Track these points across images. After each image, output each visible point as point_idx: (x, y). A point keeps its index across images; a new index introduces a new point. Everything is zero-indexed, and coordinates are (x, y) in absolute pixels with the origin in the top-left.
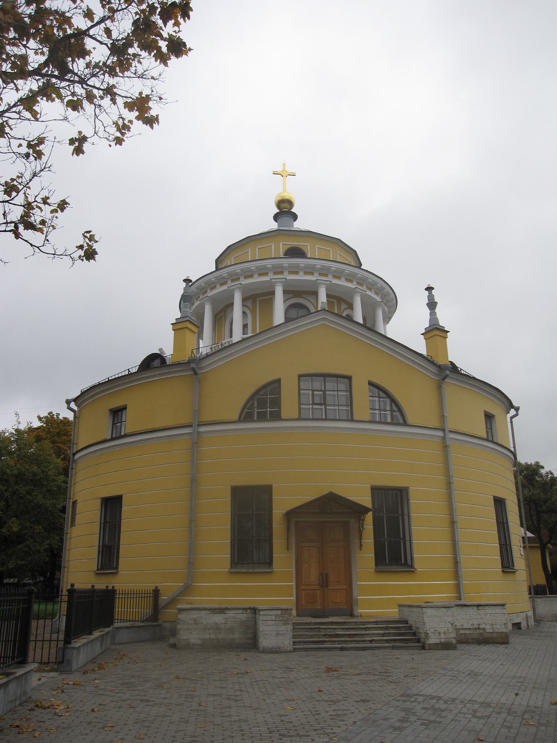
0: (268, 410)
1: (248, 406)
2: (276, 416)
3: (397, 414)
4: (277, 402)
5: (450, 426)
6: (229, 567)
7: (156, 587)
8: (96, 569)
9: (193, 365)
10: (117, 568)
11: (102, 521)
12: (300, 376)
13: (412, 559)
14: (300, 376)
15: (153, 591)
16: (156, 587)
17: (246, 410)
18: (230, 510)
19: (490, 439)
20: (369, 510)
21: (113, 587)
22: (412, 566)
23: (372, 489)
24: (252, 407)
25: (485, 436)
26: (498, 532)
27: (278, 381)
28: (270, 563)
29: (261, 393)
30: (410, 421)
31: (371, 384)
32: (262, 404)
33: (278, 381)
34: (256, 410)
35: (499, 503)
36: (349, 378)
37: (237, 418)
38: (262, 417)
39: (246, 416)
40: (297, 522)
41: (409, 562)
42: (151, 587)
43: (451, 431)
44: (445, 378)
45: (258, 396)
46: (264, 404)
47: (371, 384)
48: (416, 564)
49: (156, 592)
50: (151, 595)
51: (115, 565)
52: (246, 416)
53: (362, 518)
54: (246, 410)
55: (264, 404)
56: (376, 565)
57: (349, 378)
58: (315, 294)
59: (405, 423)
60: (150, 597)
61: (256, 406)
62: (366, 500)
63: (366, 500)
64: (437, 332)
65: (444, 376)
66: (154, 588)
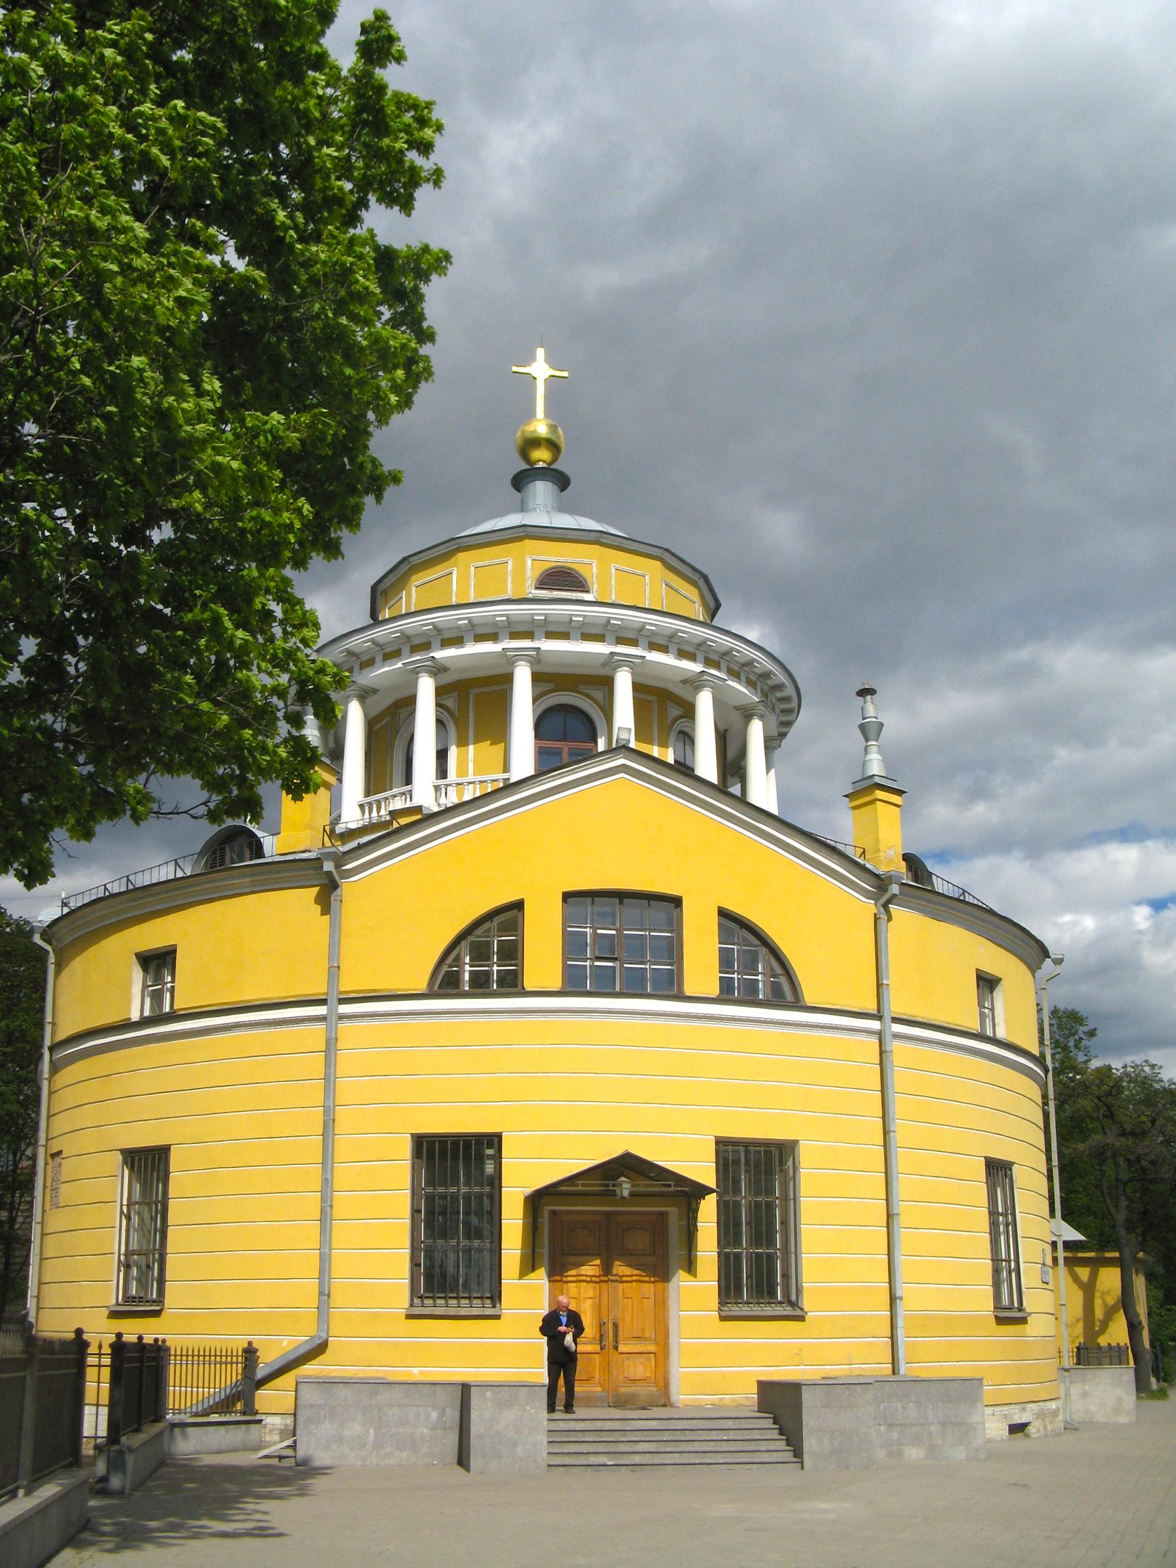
0: (495, 968)
1: (449, 960)
2: (512, 984)
3: (783, 980)
4: (513, 953)
5: (897, 1005)
6: (407, 1305)
7: (250, 1343)
8: (114, 1302)
9: (328, 866)
10: (160, 1300)
11: (125, 1202)
12: (567, 896)
13: (799, 1291)
14: (567, 896)
15: (246, 1351)
16: (250, 1343)
17: (445, 968)
18: (408, 1184)
19: (989, 1033)
20: (709, 1191)
21: (164, 1341)
22: (794, 1305)
23: (717, 1143)
24: (458, 960)
25: (974, 1026)
26: (990, 1233)
27: (519, 905)
28: (496, 1297)
29: (479, 931)
30: (809, 999)
31: (723, 913)
32: (480, 953)
33: (519, 905)
34: (467, 968)
35: (998, 1171)
36: (677, 902)
37: (422, 985)
38: (480, 985)
39: (445, 982)
40: (554, 1213)
41: (793, 1298)
42: (240, 1343)
43: (896, 1020)
44: (889, 901)
45: (471, 938)
46: (484, 956)
47: (723, 913)
48: (807, 1302)
49: (250, 1353)
50: (240, 1359)
51: (154, 1296)
52: (445, 982)
53: (694, 1206)
54: (445, 968)
55: (484, 956)
56: (722, 1303)
57: (677, 902)
58: (607, 684)
59: (797, 1004)
60: (237, 1363)
61: (467, 960)
62: (705, 1172)
63: (705, 1172)
64: (879, 794)
65: (887, 896)
66: (246, 1345)
